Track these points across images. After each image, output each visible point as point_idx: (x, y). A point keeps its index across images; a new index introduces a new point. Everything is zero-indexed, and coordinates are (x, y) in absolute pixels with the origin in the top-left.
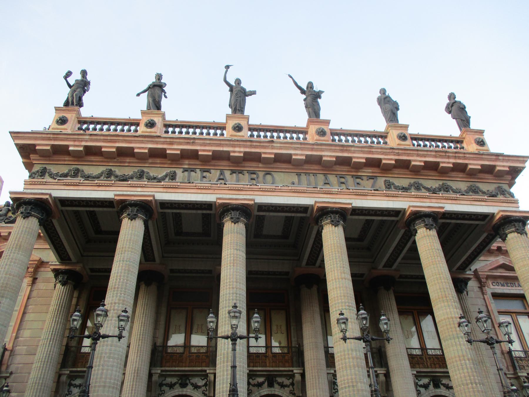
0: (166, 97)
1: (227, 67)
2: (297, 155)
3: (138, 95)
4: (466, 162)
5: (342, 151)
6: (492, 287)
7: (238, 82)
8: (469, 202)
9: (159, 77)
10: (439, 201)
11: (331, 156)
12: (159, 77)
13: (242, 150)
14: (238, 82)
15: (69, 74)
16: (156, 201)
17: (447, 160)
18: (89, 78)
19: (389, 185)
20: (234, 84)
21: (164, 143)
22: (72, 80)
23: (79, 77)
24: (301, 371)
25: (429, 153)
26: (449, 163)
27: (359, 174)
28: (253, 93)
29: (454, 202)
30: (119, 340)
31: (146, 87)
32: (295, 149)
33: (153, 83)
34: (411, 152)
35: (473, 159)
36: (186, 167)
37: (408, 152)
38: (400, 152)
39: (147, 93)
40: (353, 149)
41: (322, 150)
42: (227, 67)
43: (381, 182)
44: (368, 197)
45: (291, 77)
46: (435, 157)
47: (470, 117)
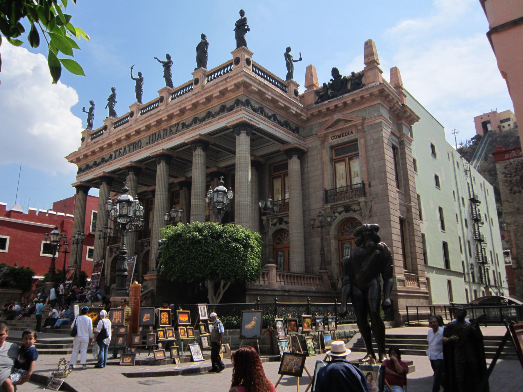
1: (132, 68)
2: (142, 128)
4: (211, 93)
5: (157, 116)
6: (331, 141)
8: (216, 122)
9: (113, 90)
10: (202, 128)
11: (154, 122)
12: (113, 90)
13: (124, 134)
16: (108, 173)
17: (201, 97)
19: (184, 125)
20: (138, 77)
21: (102, 143)
25: (192, 97)
26: (203, 99)
27: (172, 124)
29: (209, 125)
32: (141, 124)
34: (184, 101)
35: (215, 89)
36: (115, 150)
37: (183, 102)
38: (180, 104)
40: (160, 113)
41: (150, 120)
42: (132, 68)
43: (180, 126)
44: (173, 140)
45: (156, 58)
46: (196, 98)
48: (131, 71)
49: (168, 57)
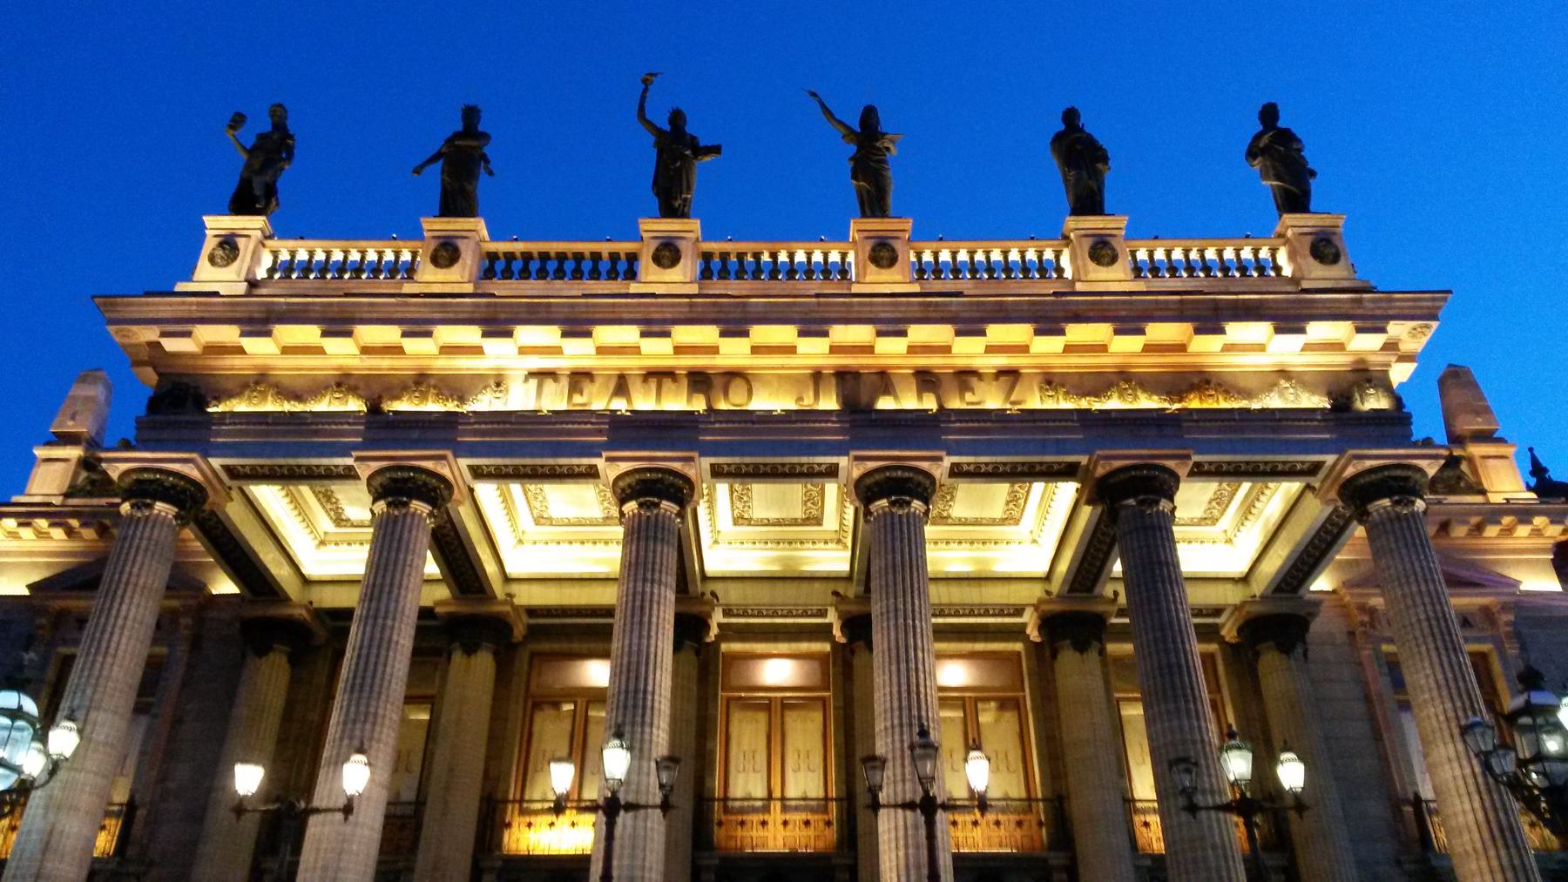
0: (491, 173)
3: (417, 171)
7: (677, 117)
9: (471, 114)
12: (471, 114)
14: (677, 117)
15: (238, 121)
18: (292, 126)
20: (667, 128)
22: (248, 135)
23: (266, 127)
24: (848, 862)
28: (716, 150)
30: (346, 819)
31: (436, 145)
33: (457, 135)
39: (438, 166)
45: (814, 94)
47: (1313, 173)
48: (645, 90)
49: (869, 116)
